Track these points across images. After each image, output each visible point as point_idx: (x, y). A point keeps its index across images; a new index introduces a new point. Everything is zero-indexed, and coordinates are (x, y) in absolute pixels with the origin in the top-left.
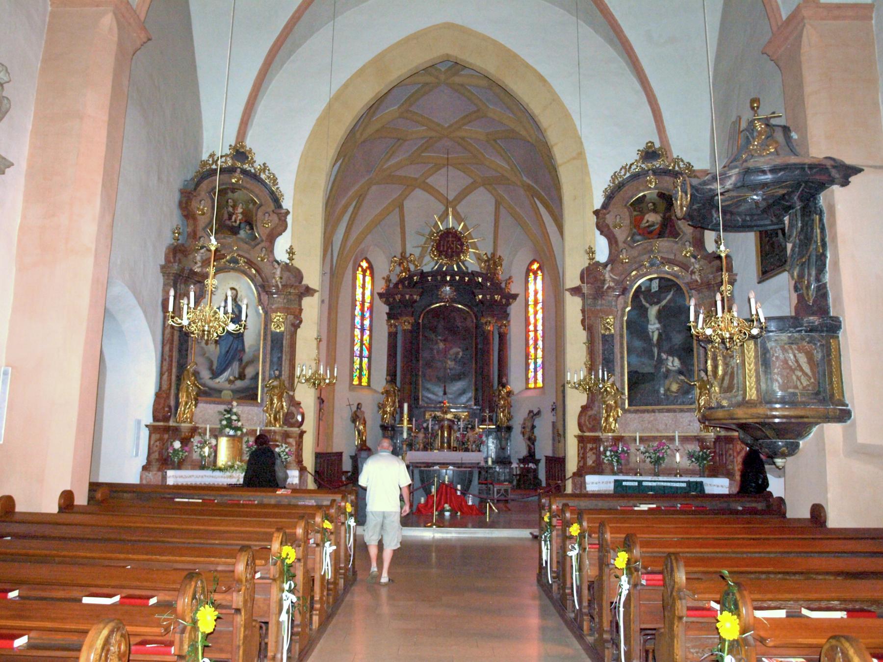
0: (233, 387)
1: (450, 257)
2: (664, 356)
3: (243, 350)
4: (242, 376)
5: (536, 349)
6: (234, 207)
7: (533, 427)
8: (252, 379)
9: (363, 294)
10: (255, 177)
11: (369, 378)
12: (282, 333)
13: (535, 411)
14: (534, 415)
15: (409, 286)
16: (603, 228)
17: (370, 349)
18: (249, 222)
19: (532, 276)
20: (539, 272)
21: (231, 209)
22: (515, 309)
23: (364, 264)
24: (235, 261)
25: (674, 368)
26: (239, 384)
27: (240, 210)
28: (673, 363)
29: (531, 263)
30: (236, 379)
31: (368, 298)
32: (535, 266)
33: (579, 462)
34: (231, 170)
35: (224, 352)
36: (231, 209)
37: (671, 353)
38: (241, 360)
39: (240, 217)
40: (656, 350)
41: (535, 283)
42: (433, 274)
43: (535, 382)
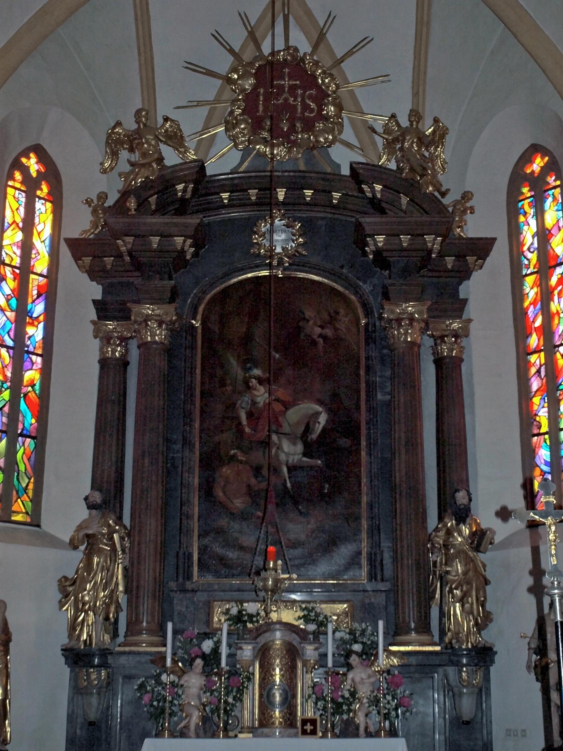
9: (26, 247)
11: (37, 500)
15: (161, 209)
17: (42, 412)
23: (33, 165)
29: (526, 158)
31: (41, 264)
32: (538, 164)
42: (237, 185)
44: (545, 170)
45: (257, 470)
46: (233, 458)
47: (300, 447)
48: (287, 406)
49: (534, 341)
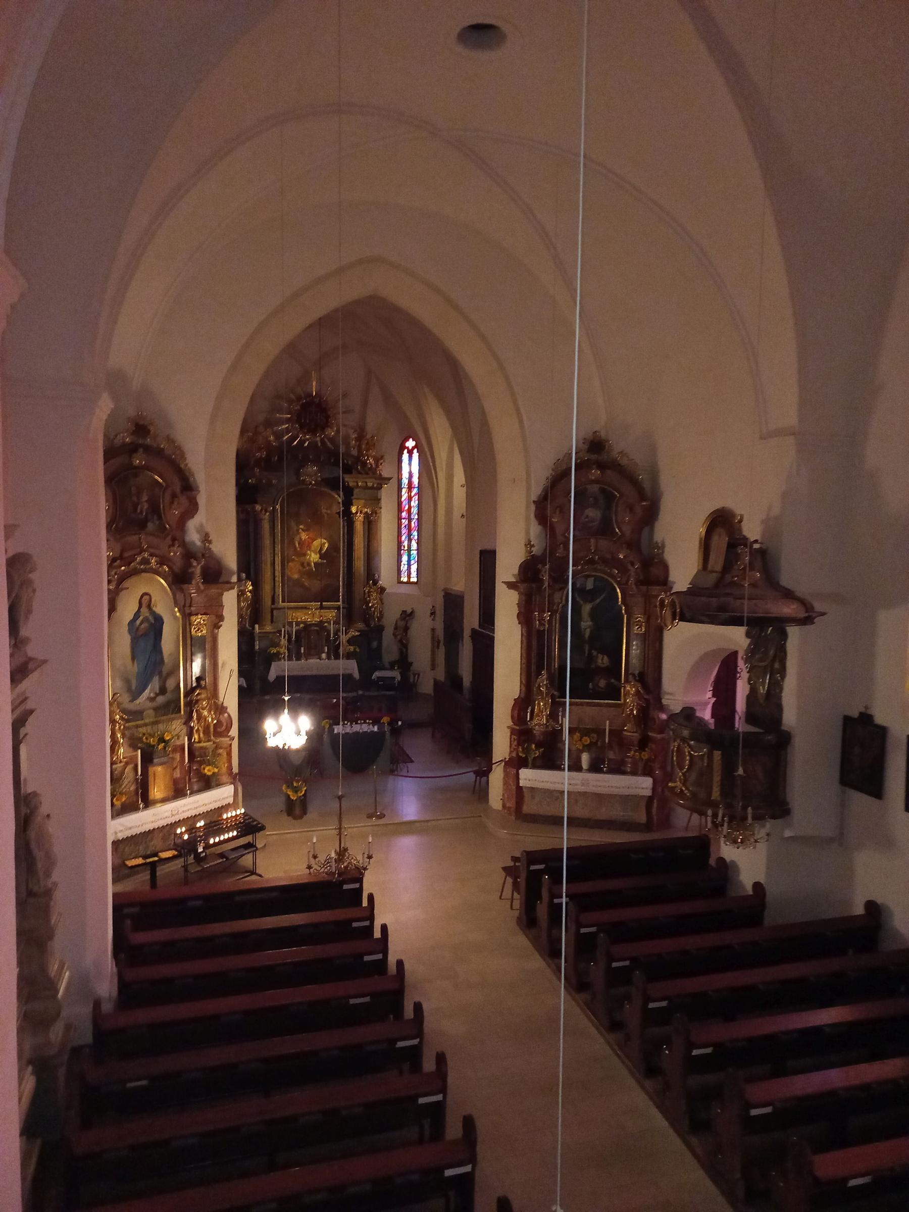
0: (154, 704)
1: (313, 432)
2: (595, 653)
4: (163, 691)
5: (410, 540)
6: (139, 495)
7: (406, 629)
8: (173, 691)
10: (159, 453)
12: (203, 638)
13: (409, 611)
14: (407, 616)
16: (542, 517)
18: (155, 510)
19: (405, 456)
20: (415, 451)
21: (135, 499)
22: (386, 495)
24: (146, 562)
25: (603, 666)
27: (145, 498)
28: (603, 661)
30: (157, 695)
32: (410, 444)
33: (511, 752)
34: (133, 449)
36: (135, 499)
37: (602, 651)
38: (160, 673)
39: (146, 506)
40: (587, 648)
41: (410, 464)
43: (409, 576)
44: (413, 448)
45: (302, 564)
46: (293, 560)
47: (318, 556)
48: (314, 540)
49: (404, 514)
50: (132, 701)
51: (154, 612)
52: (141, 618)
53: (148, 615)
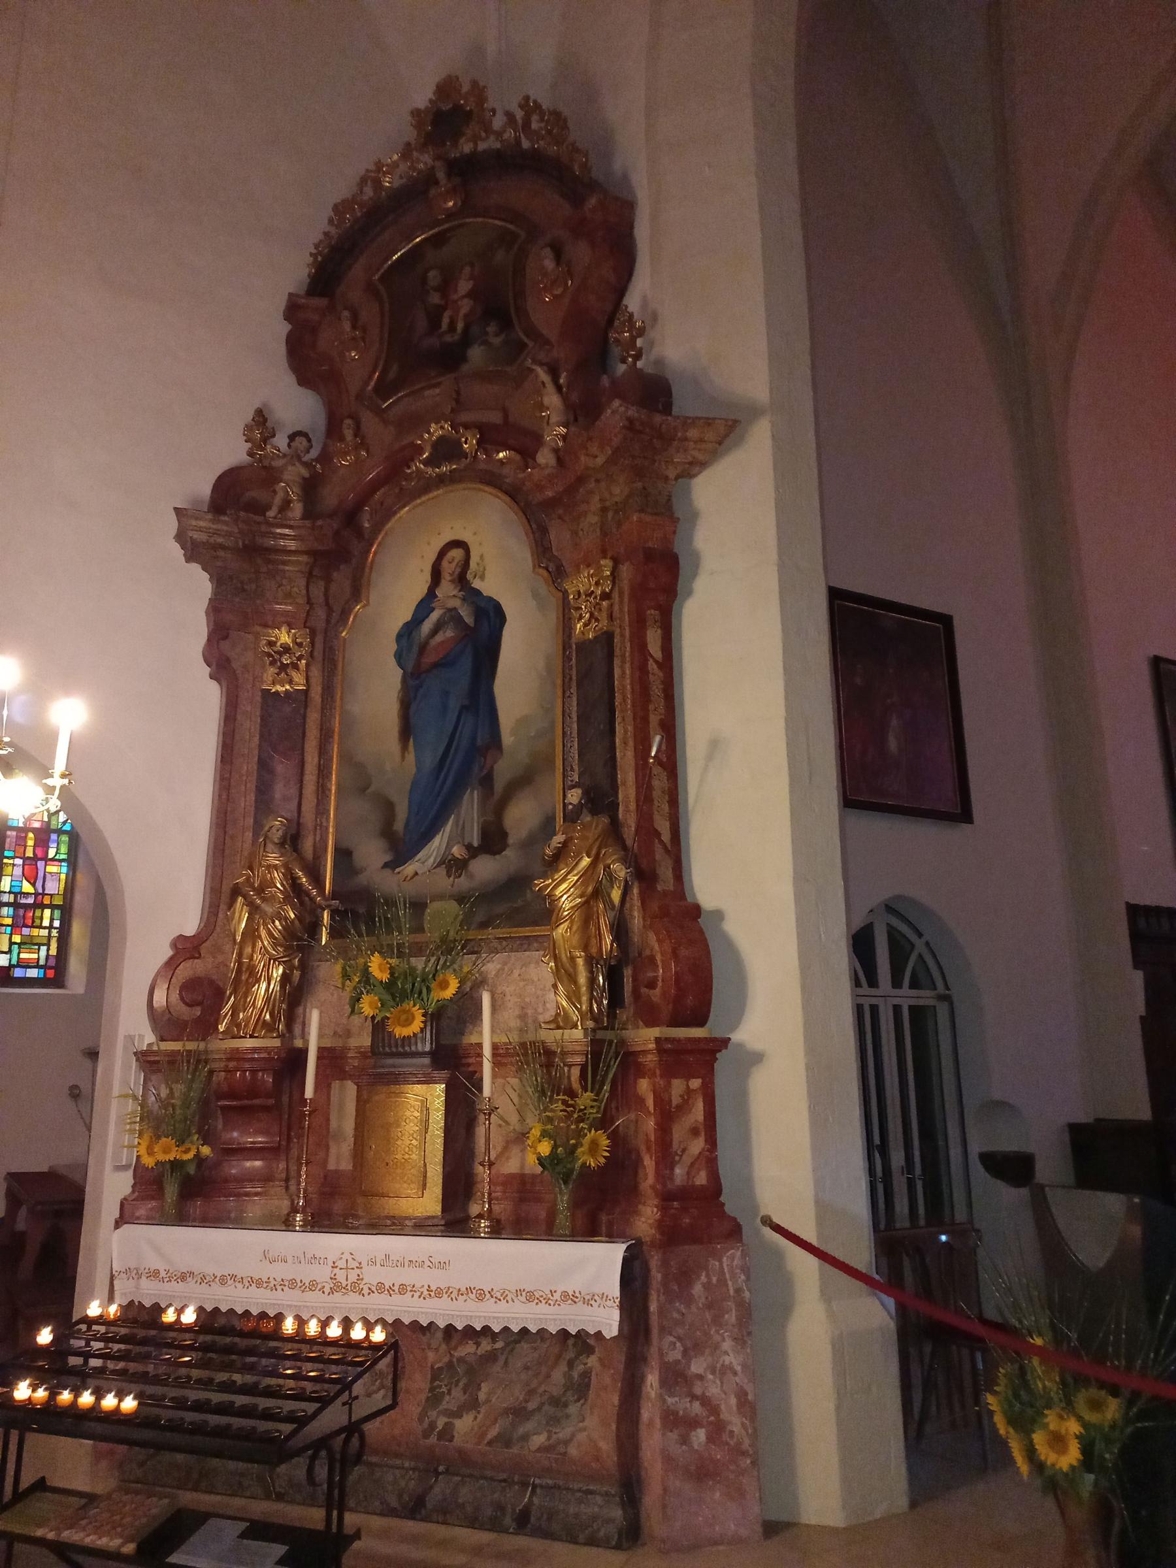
0: (463, 883)
3: (495, 741)
4: (493, 840)
6: (446, 287)
18: (499, 307)
21: (435, 299)
26: (485, 869)
27: (464, 286)
30: (473, 852)
35: (430, 761)
36: (435, 299)
38: (487, 781)
50: (392, 865)
51: (477, 593)
52: (435, 616)
53: (456, 603)
